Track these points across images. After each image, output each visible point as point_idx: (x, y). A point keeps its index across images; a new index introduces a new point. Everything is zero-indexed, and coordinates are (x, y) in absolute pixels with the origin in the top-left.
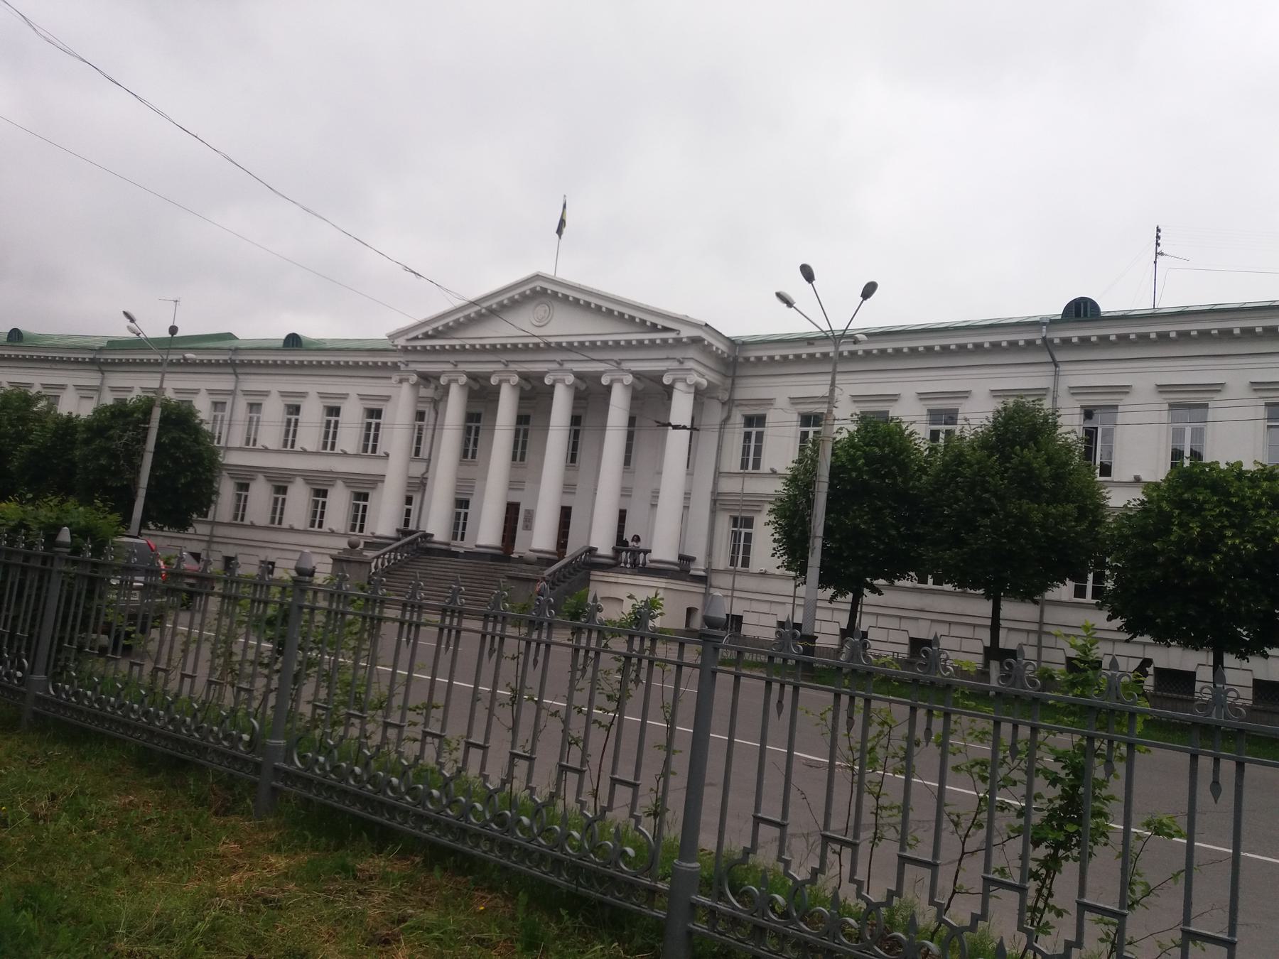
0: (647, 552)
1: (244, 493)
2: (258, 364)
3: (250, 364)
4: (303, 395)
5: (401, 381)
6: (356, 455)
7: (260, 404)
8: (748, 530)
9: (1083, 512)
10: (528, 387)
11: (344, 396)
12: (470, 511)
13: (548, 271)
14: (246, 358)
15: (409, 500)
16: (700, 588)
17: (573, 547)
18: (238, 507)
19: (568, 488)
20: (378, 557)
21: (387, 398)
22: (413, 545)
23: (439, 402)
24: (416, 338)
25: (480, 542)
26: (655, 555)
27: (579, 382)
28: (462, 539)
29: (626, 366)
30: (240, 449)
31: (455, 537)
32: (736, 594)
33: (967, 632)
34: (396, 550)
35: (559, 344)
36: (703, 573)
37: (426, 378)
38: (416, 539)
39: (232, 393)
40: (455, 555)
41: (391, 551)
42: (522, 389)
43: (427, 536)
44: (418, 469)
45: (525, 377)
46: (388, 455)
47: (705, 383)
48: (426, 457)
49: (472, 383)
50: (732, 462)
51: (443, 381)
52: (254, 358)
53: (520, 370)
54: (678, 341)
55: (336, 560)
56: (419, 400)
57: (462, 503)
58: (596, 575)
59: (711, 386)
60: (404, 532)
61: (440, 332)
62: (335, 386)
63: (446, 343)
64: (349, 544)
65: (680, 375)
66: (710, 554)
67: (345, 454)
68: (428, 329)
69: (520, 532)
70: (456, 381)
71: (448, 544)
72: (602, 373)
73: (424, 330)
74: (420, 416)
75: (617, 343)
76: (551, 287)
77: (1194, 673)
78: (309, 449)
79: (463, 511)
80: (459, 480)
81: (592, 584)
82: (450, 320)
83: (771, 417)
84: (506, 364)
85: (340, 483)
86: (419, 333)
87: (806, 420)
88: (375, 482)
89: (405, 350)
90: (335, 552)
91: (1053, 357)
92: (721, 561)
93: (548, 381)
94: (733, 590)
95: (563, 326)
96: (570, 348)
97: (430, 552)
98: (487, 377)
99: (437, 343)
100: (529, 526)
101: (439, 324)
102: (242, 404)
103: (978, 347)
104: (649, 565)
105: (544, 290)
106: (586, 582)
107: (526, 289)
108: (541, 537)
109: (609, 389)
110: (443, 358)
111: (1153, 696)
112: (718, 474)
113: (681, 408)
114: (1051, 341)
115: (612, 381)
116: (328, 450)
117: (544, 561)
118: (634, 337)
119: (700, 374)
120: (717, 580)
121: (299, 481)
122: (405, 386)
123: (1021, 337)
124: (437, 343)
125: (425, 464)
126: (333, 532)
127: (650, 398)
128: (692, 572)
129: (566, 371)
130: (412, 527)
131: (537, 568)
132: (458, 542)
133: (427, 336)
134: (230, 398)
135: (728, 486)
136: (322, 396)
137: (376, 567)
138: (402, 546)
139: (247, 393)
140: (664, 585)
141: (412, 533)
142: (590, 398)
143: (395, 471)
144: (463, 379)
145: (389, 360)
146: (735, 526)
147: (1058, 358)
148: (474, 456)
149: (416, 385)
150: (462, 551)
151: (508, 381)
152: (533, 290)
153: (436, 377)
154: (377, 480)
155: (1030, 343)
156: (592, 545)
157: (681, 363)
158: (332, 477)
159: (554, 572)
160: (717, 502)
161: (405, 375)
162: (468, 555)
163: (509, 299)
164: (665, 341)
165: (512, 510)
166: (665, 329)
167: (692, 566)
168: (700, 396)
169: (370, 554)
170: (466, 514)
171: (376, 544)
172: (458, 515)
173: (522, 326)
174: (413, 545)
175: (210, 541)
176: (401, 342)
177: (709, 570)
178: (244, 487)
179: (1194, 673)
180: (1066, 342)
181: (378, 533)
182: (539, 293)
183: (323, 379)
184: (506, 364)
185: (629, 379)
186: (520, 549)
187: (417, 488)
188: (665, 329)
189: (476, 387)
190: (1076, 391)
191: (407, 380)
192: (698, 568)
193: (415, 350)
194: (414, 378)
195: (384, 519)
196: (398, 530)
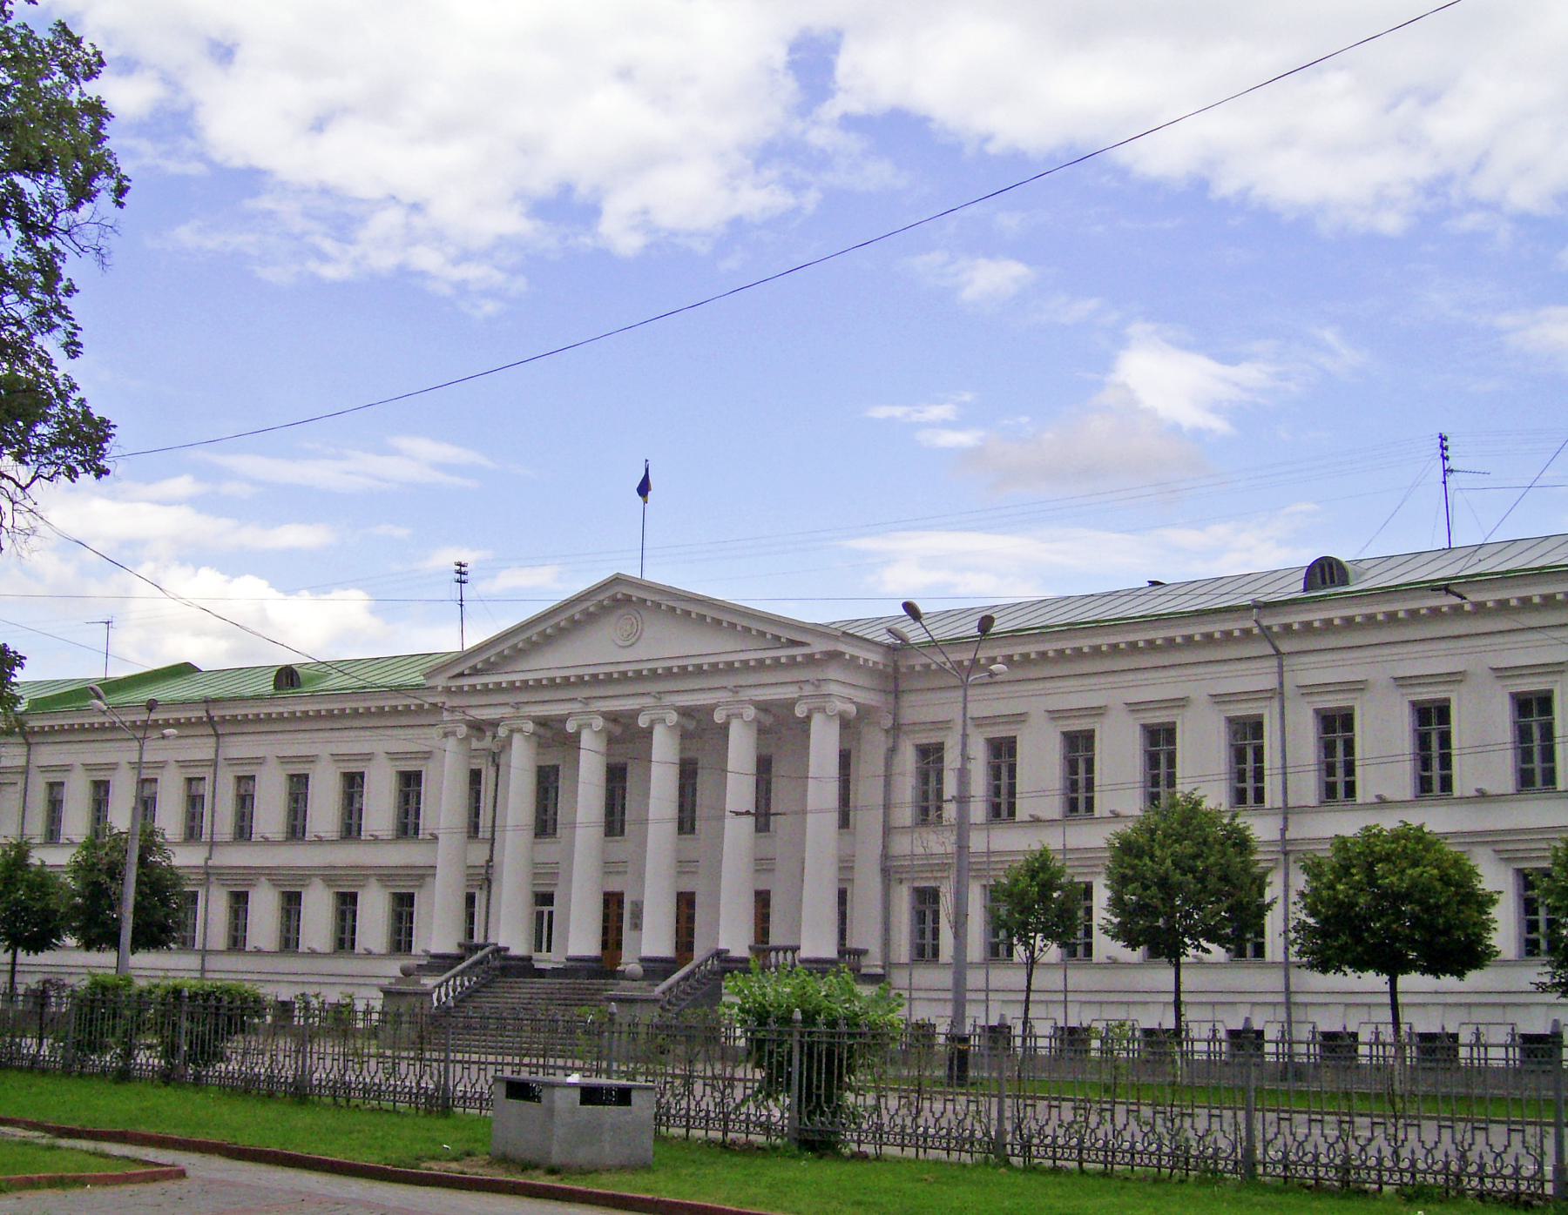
2: (246, 720)
3: (234, 720)
4: (311, 759)
5: (446, 735)
6: (388, 841)
7: (253, 778)
11: (368, 757)
12: (556, 908)
13: (634, 573)
14: (228, 713)
15: (470, 900)
17: (700, 951)
19: (684, 865)
20: (440, 986)
21: (427, 755)
23: (495, 759)
24: (462, 675)
28: (549, 950)
31: (539, 948)
32: (915, 994)
34: (462, 973)
35: (699, 667)
36: (880, 971)
37: (478, 727)
38: (486, 956)
40: (541, 973)
41: (454, 977)
43: (499, 951)
44: (478, 854)
45: (612, 718)
46: (436, 838)
47: (852, 709)
48: (488, 835)
49: (541, 731)
50: (905, 815)
51: (502, 732)
52: (240, 711)
55: (388, 993)
56: (473, 754)
57: (545, 899)
59: (864, 712)
60: (469, 948)
63: (504, 679)
66: (886, 942)
69: (627, 934)
71: (530, 959)
73: (471, 663)
74: (475, 776)
75: (745, 663)
79: (546, 909)
80: (535, 865)
84: (517, 706)
86: (464, 667)
88: (422, 877)
89: (448, 690)
90: (386, 981)
91: (1275, 648)
92: (903, 950)
93: (719, 717)
94: (987, 991)
95: (665, 645)
99: (491, 679)
100: (637, 926)
105: (628, 599)
109: (725, 728)
110: (638, 688)
112: (888, 830)
113: (824, 743)
114: (1269, 628)
115: (653, 723)
117: (656, 969)
118: (767, 655)
120: (899, 979)
121: (318, 884)
123: (1235, 625)
124: (491, 679)
125: (488, 847)
127: (781, 732)
128: (864, 971)
129: (663, 707)
130: (478, 938)
131: (644, 984)
132: (544, 954)
133: (475, 672)
135: (902, 845)
136: (337, 758)
137: (439, 1000)
138: (470, 967)
141: (482, 947)
143: (446, 857)
146: (993, 900)
147: (1285, 647)
149: (467, 738)
150: (549, 966)
152: (614, 599)
153: (495, 724)
154: (424, 874)
156: (722, 946)
159: (670, 989)
160: (889, 872)
161: (450, 727)
162: (556, 973)
163: (582, 612)
165: (612, 903)
168: (847, 725)
169: (429, 982)
170: (551, 913)
171: (441, 963)
172: (540, 915)
176: (440, 681)
177: (888, 964)
180: (1287, 628)
181: (433, 951)
186: (629, 962)
187: (481, 882)
188: (793, 643)
189: (618, 730)
191: (454, 734)
192: (872, 964)
194: (463, 730)
195: (437, 932)
196: (460, 945)
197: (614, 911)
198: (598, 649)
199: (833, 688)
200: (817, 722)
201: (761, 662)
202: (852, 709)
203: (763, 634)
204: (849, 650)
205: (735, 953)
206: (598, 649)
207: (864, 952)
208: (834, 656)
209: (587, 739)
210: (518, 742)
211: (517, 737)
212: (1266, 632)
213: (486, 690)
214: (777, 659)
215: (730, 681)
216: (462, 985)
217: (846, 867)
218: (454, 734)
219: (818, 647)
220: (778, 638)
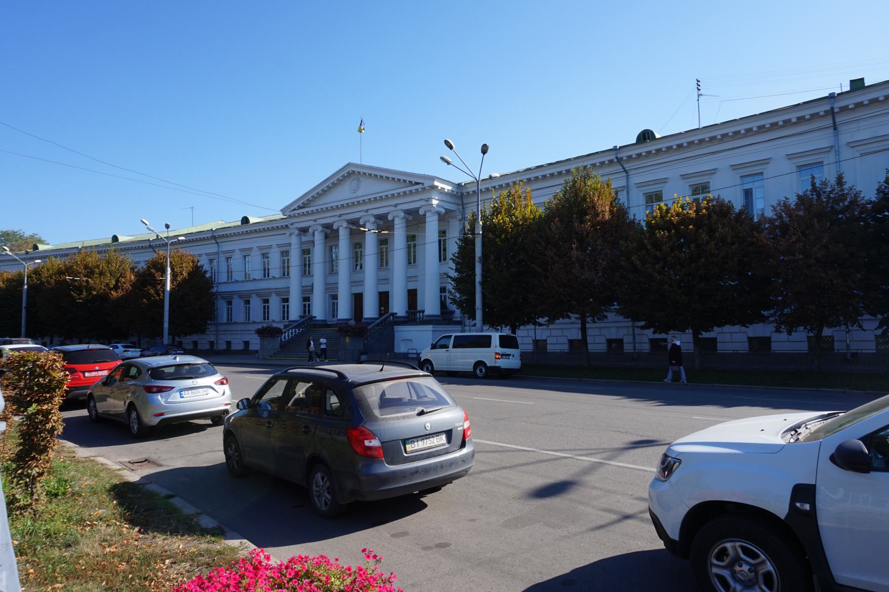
0: (423, 312)
13: (358, 162)
25: (339, 317)
26: (426, 313)
30: (225, 283)
39: (217, 253)
51: (311, 231)
58: (397, 328)
62: (264, 242)
68: (300, 203)
82: (309, 197)
86: (295, 206)
89: (290, 216)
95: (368, 189)
101: (304, 200)
102: (223, 259)
104: (425, 318)
107: (345, 173)
108: (370, 310)
114: (622, 158)
122: (293, 236)
123: (606, 159)
124: (304, 210)
133: (300, 208)
139: (224, 252)
144: (320, 228)
155: (611, 162)
158: (269, 292)
164: (417, 190)
166: (417, 183)
173: (343, 194)
176: (288, 213)
180: (630, 157)
182: (350, 174)
190: (639, 185)
194: (297, 232)
197: (358, 300)
198: (343, 194)
201: (405, 193)
205: (399, 314)
209: (397, 222)
210: (316, 234)
212: (620, 160)
213: (303, 214)
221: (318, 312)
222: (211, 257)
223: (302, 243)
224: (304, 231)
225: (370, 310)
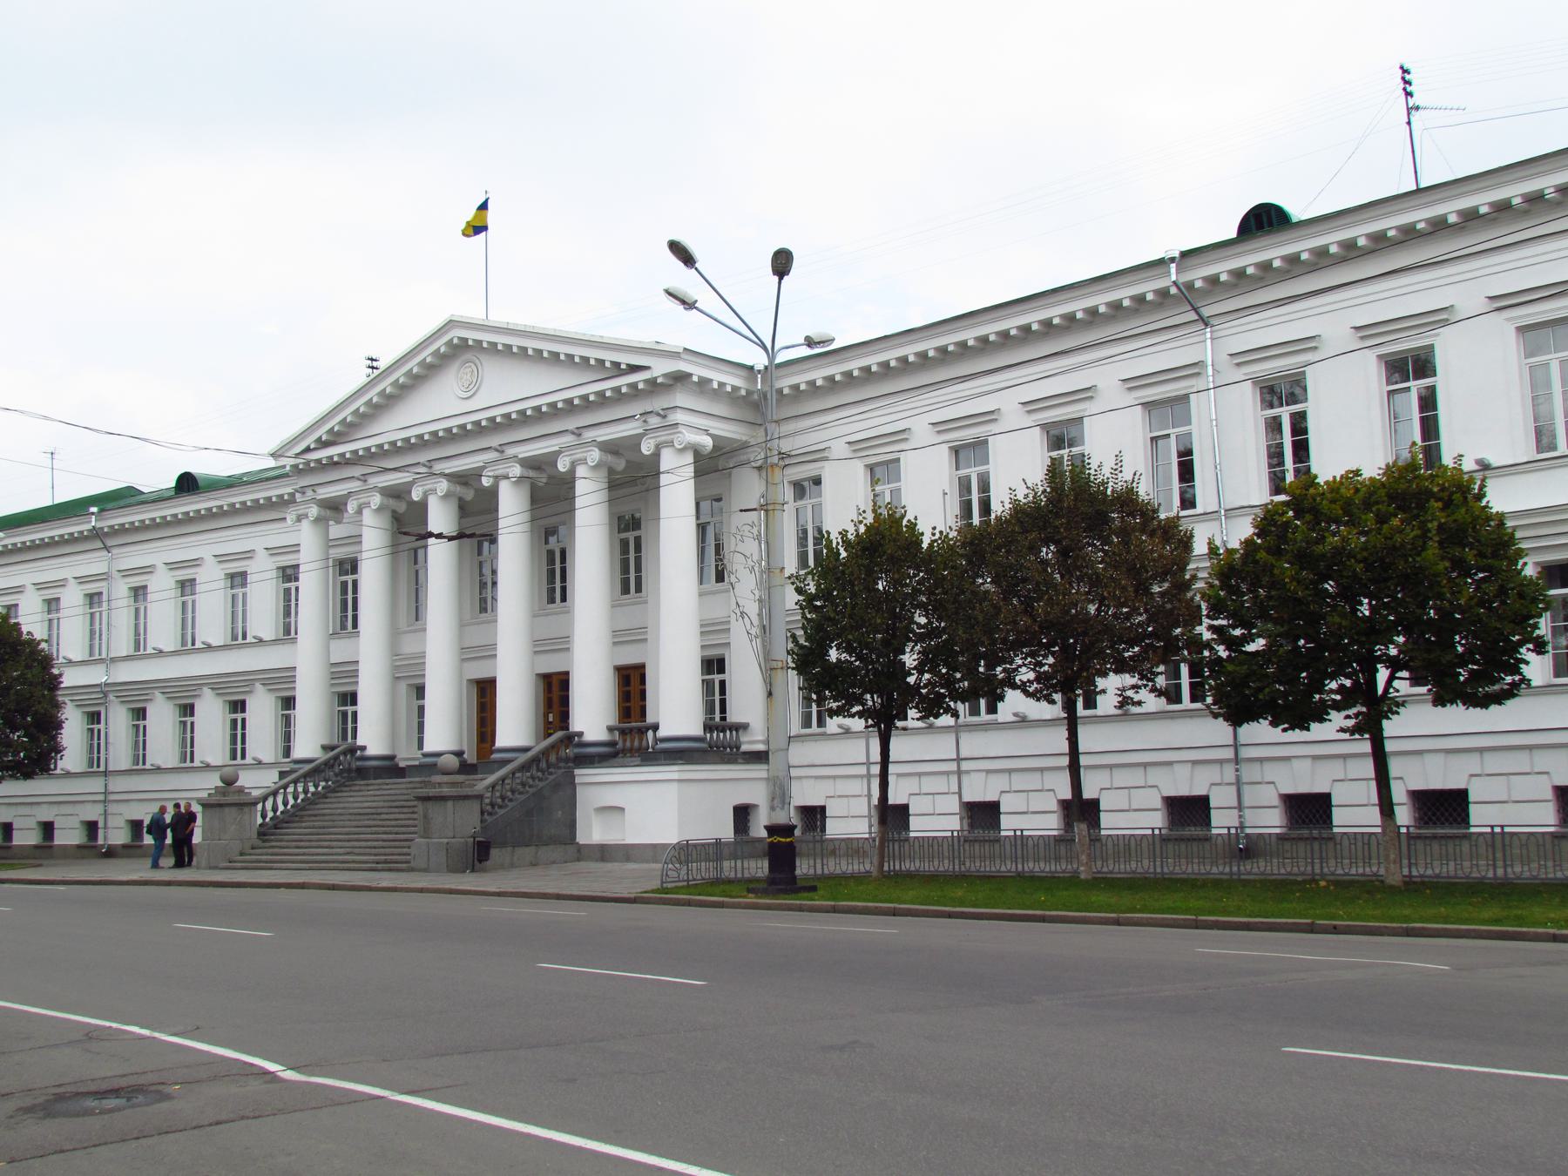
0: (655, 727)
1: (141, 723)
4: (195, 563)
5: (299, 519)
6: (275, 641)
8: (721, 677)
9: (1454, 536)
10: (620, 465)
16: (759, 771)
18: (184, 744)
22: (345, 766)
24: (308, 450)
26: (663, 732)
27: (610, 458)
29: (438, 467)
33: (1033, 781)
36: (761, 747)
39: (104, 577)
41: (295, 782)
42: (611, 471)
49: (392, 502)
51: (351, 507)
53: (463, 469)
54: (652, 382)
58: (583, 775)
61: (339, 434)
64: (223, 780)
65: (663, 436)
67: (260, 641)
68: (322, 432)
70: (584, 461)
72: (557, 453)
76: (472, 335)
77: (1329, 795)
78: (215, 643)
81: (579, 790)
82: (346, 413)
83: (828, 472)
85: (207, 691)
86: (310, 441)
87: (958, 452)
90: (204, 794)
95: (505, 388)
96: (509, 423)
97: (362, 773)
98: (477, 474)
101: (333, 423)
102: (121, 589)
103: (1471, 217)
106: (568, 787)
107: (440, 344)
108: (515, 726)
111: (1164, 840)
116: (240, 641)
119: (698, 425)
122: (305, 524)
124: (333, 451)
126: (260, 763)
128: (744, 748)
134: (104, 584)
139: (127, 573)
140: (675, 776)
142: (551, 497)
145: (274, 491)
148: (639, 589)
149: (318, 520)
151: (584, 461)
157: (664, 417)
158: (248, 680)
167: (744, 738)
174: (345, 766)
175: (106, 798)
176: (288, 462)
178: (140, 714)
179: (1329, 795)
182: (455, 349)
183: (193, 538)
184: (364, 478)
185: (595, 455)
191: (306, 516)
193: (322, 466)
194: (314, 511)
199: (679, 417)
200: (668, 460)
202: (708, 442)
203: (601, 362)
204: (697, 371)
206: (441, 404)
207: (744, 727)
208: (680, 378)
210: (368, 517)
211: (366, 512)
213: (332, 464)
214: (617, 390)
215: (572, 423)
216: (306, 791)
217: (712, 629)
218: (306, 516)
219: (660, 368)
220: (616, 365)
221: (372, 738)
222: (92, 588)
223: (329, 543)
224: (335, 507)
225: (515, 726)
